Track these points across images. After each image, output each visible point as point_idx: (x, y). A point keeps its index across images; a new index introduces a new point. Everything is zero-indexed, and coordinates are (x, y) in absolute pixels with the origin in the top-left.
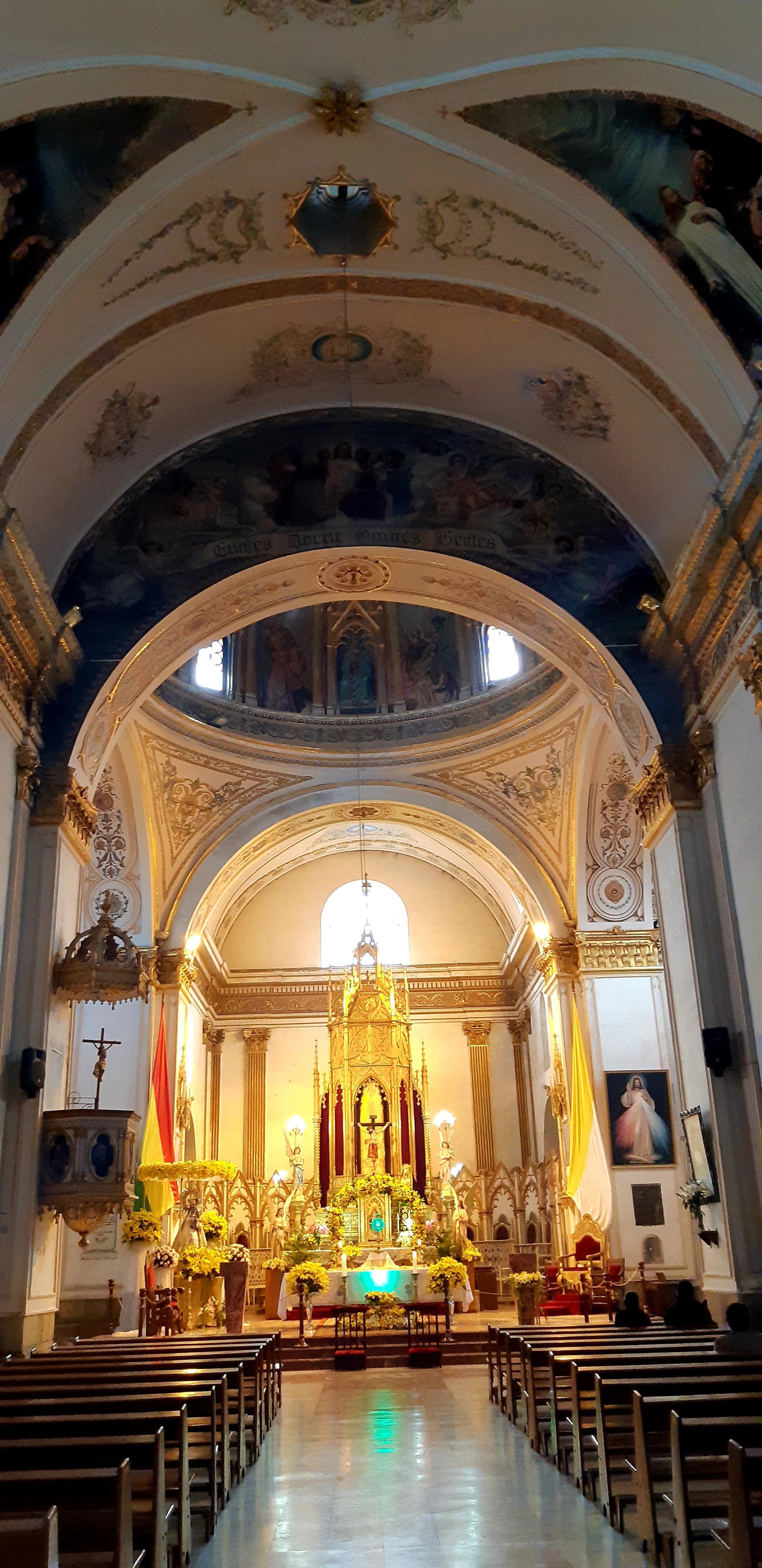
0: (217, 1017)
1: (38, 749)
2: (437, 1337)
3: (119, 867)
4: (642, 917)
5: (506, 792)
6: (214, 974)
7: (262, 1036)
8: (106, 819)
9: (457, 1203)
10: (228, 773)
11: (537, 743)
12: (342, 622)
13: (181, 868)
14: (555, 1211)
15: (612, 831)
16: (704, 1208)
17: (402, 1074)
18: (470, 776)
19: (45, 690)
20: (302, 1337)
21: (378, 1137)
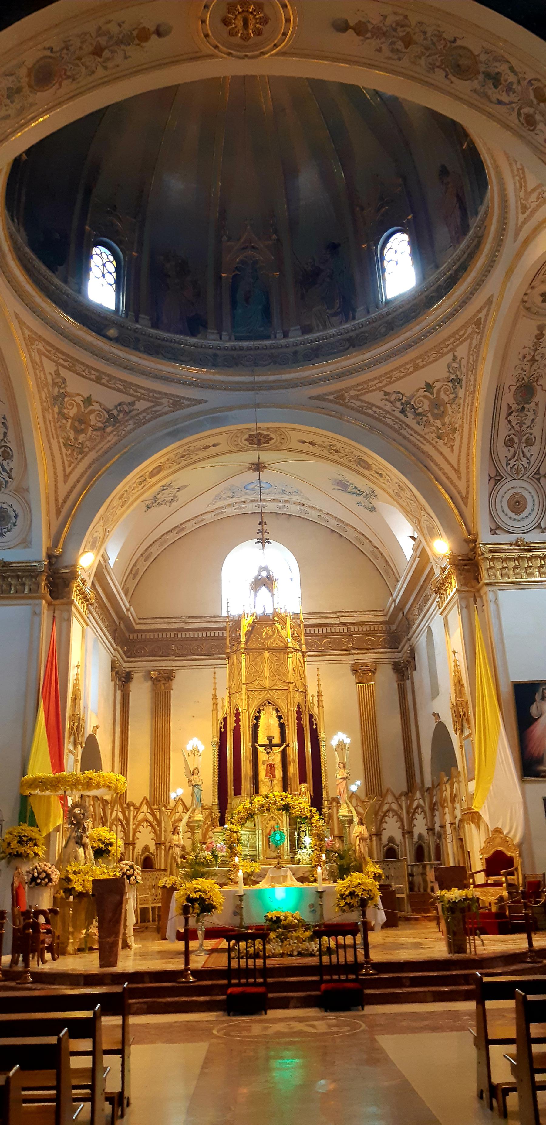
0: (126, 659)
2: (355, 967)
3: (7, 479)
5: (403, 412)
6: (123, 618)
7: (168, 676)
9: (356, 819)
11: (438, 352)
13: (74, 486)
14: (445, 831)
15: (516, 440)
17: (298, 698)
18: (367, 397)
20: (187, 969)
21: (276, 757)
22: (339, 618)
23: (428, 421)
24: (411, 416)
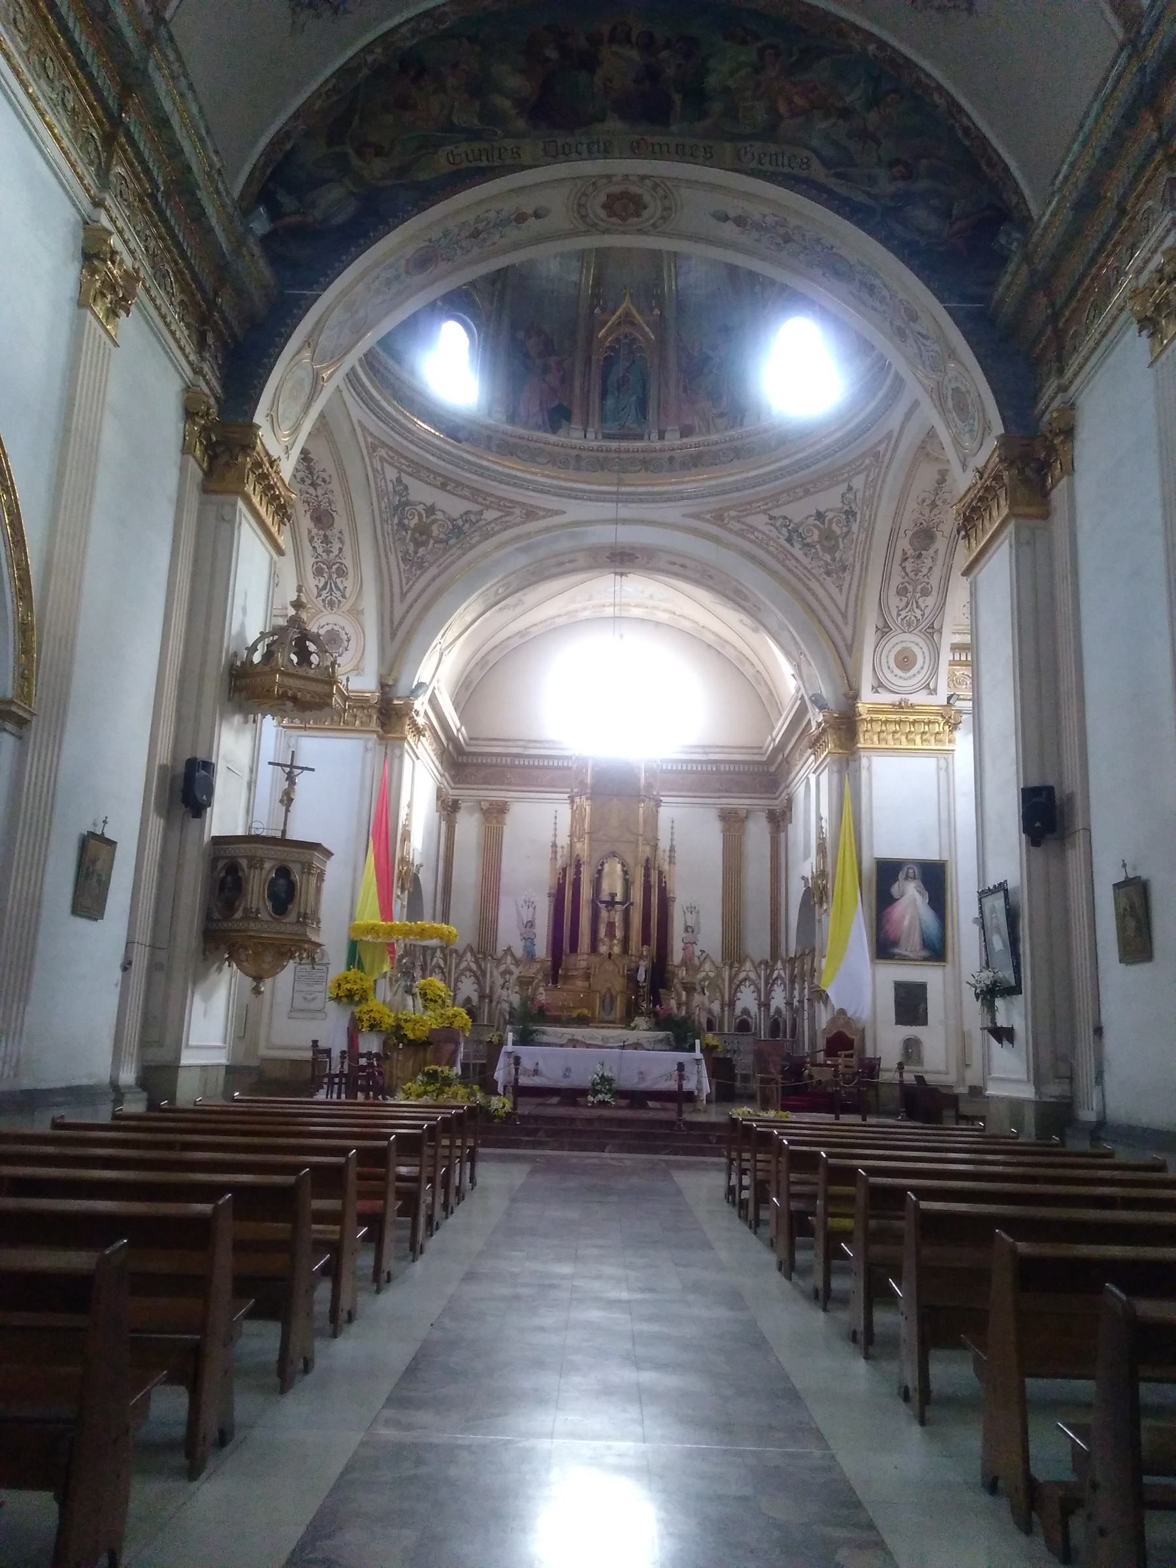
0: (453, 785)
1: (217, 399)
3: (340, 598)
4: (935, 690)
5: (789, 540)
6: (451, 738)
8: (326, 540)
10: (468, 499)
12: (610, 327)
13: (411, 606)
15: (910, 588)
16: (999, 1003)
17: (647, 851)
18: (750, 520)
19: (225, 320)
21: (618, 918)
22: (705, 753)
23: (817, 553)
24: (797, 546)
